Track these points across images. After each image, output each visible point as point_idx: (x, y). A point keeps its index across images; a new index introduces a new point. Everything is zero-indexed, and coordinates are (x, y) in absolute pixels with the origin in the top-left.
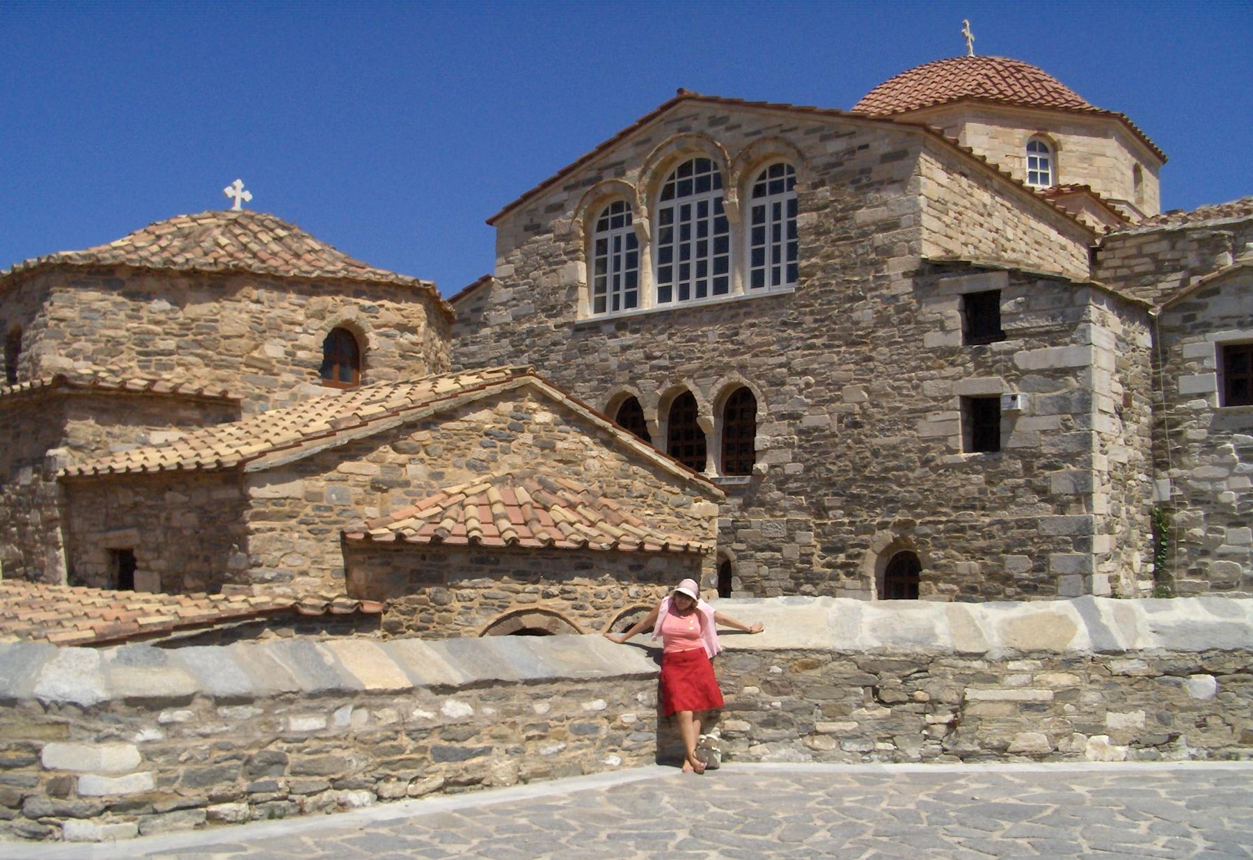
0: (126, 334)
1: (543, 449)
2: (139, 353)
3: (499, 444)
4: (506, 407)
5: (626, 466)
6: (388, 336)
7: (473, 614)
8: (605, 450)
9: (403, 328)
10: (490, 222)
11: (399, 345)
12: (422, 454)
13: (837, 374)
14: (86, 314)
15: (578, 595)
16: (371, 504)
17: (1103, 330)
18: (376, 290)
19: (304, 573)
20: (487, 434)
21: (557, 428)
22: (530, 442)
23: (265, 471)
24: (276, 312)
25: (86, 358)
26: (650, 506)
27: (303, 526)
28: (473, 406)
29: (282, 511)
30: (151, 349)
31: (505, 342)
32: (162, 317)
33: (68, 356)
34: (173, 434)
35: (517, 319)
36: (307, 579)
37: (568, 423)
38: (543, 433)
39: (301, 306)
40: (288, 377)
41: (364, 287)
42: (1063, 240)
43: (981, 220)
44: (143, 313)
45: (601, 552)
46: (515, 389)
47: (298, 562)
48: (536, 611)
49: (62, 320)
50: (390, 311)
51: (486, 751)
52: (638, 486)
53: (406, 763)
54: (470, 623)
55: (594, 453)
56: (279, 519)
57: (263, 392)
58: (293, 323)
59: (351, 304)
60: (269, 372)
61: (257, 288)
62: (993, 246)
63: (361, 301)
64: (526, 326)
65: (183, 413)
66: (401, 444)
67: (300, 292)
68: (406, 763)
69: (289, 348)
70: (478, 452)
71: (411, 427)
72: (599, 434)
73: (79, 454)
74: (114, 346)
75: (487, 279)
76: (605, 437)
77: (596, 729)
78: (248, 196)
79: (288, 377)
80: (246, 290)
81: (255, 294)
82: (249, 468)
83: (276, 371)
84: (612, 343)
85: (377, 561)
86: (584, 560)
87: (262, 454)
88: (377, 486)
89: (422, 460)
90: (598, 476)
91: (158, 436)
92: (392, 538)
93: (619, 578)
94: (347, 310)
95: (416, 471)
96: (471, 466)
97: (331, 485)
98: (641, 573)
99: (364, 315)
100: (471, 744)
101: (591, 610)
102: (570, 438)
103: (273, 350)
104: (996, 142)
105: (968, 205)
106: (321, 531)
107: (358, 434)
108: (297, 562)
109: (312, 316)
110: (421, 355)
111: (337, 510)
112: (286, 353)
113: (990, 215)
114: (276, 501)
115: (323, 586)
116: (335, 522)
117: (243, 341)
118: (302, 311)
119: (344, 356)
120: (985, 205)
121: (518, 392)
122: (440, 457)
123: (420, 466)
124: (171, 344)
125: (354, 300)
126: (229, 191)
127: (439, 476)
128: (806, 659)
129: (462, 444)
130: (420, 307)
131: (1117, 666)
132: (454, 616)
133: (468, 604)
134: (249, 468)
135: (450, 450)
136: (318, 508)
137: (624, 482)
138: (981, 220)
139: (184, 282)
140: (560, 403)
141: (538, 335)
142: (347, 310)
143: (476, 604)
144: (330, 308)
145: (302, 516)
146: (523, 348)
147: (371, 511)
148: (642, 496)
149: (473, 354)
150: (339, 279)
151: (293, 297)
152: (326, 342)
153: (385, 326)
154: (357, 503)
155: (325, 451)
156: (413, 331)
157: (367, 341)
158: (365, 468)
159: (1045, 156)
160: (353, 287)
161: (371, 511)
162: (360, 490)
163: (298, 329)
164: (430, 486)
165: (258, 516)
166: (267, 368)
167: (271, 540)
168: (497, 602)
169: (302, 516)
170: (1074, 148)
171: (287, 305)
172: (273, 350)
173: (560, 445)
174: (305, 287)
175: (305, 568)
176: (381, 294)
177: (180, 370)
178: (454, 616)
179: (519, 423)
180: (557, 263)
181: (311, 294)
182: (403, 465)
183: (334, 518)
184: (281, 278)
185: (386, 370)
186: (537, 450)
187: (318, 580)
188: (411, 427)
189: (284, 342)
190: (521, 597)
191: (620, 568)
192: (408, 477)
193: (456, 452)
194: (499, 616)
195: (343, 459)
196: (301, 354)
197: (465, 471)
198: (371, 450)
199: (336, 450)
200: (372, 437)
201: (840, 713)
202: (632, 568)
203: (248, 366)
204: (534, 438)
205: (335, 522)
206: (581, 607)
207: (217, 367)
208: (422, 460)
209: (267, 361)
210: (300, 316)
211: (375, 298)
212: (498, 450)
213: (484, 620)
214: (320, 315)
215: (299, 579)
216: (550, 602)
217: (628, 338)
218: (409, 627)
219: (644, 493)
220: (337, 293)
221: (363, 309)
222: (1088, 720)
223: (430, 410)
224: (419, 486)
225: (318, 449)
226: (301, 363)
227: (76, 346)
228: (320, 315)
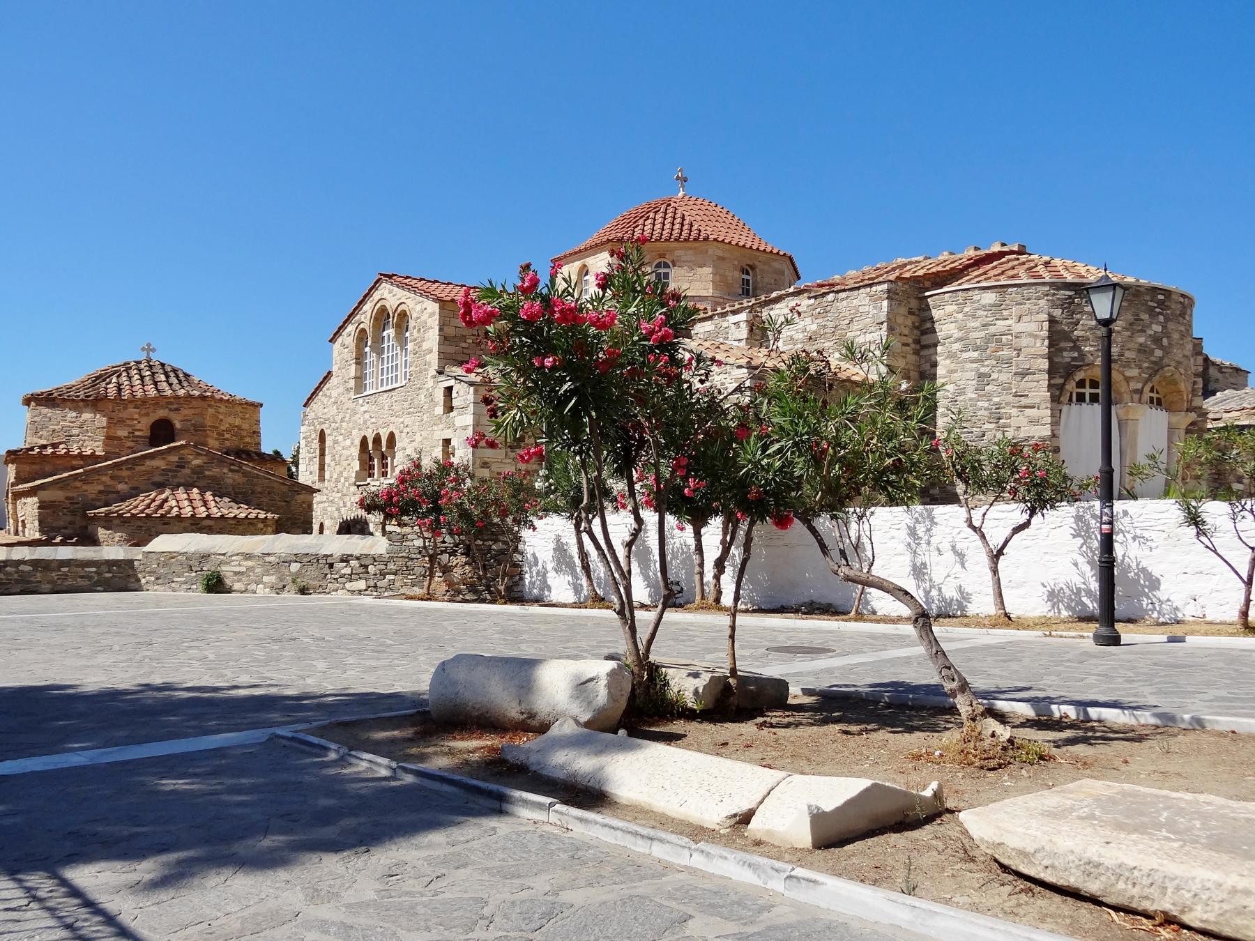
52: (259, 489)
103: (122, 433)
128: (171, 555)
131: (268, 559)
139: (81, 404)
159: (666, 270)
196: (137, 433)
210: (136, 416)
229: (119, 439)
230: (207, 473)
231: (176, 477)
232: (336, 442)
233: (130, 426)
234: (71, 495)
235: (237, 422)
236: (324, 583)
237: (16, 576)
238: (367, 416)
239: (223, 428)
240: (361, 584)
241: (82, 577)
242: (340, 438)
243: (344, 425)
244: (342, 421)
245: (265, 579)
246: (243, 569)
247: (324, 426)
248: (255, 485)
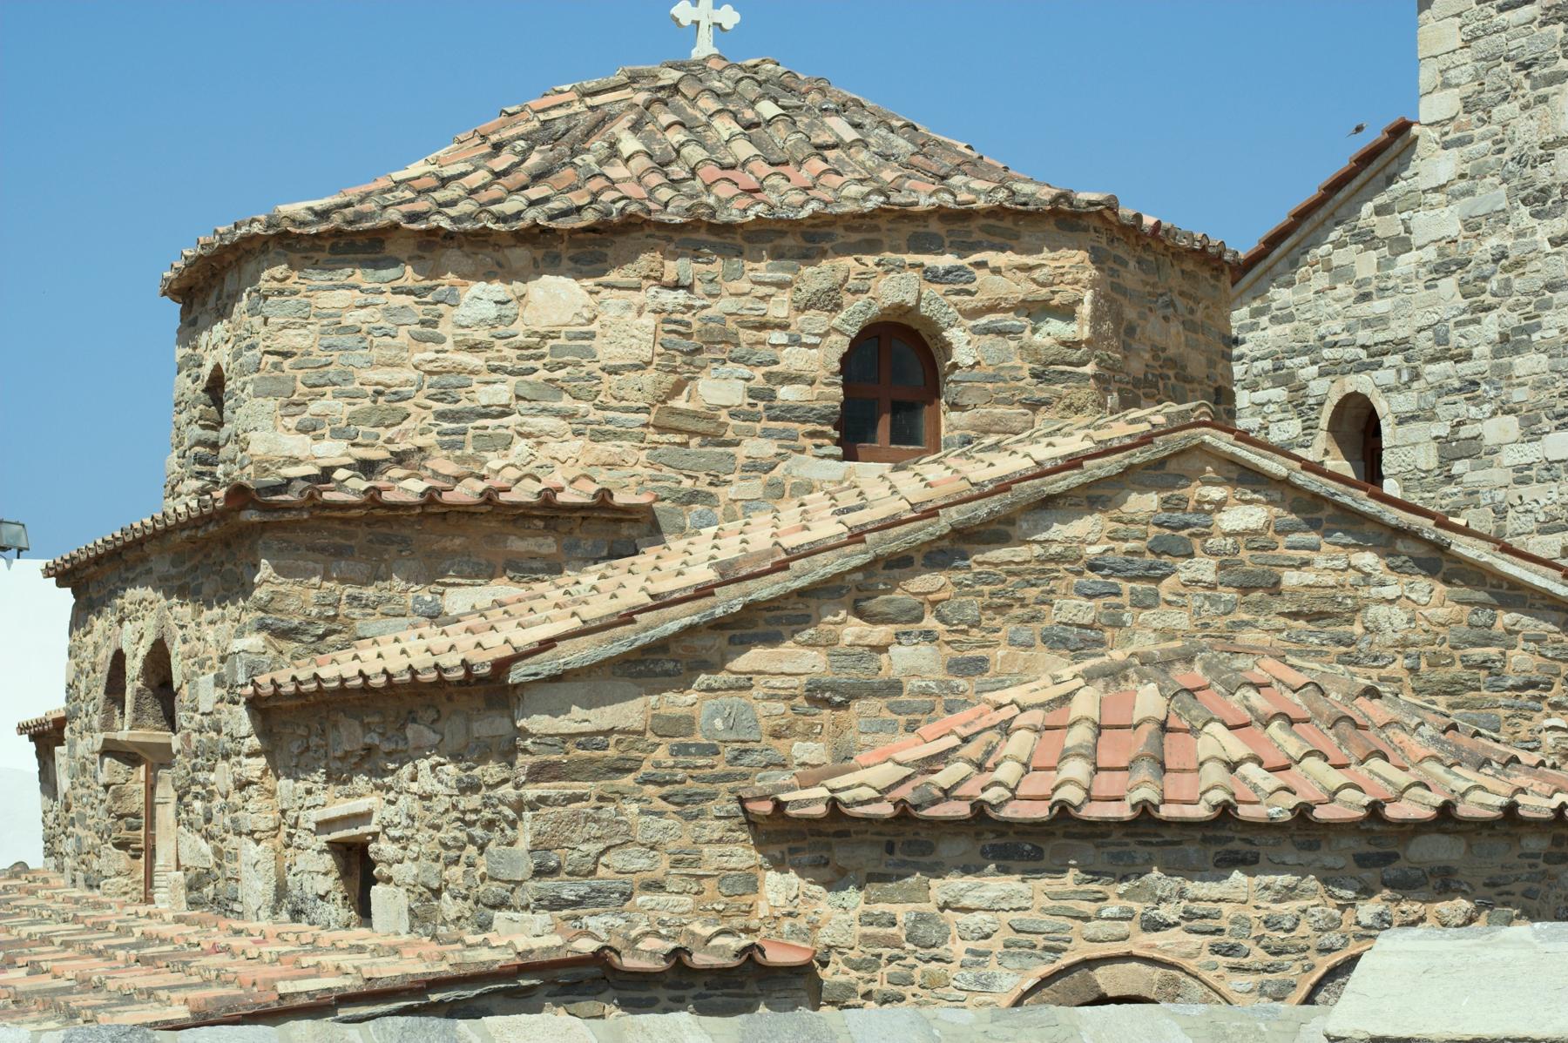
0: (414, 375)
1: (1245, 589)
2: (441, 416)
3: (1126, 587)
4: (1143, 503)
5: (1483, 617)
6: (1000, 332)
7: (992, 967)
8: (1422, 583)
9: (1037, 310)
11: (1030, 352)
12: (930, 622)
14: (334, 339)
15: (1223, 923)
16: (808, 735)
18: (961, 228)
19: (656, 886)
20: (1093, 567)
21: (1283, 541)
22: (1210, 577)
23: (554, 679)
25: (337, 434)
26: (1556, 706)
27: (650, 789)
28: (1048, 505)
30: (464, 404)
31: (1448, 285)
32: (482, 335)
33: (303, 430)
34: (502, 589)
35: (1471, 225)
36: (661, 898)
37: (1314, 525)
38: (1244, 554)
39: (781, 285)
40: (758, 448)
41: (935, 226)
44: (444, 329)
45: (1271, 826)
46: (1161, 463)
47: (643, 863)
48: (1129, 957)
49: (286, 355)
50: (1002, 274)
52: (1521, 660)
54: (986, 985)
55: (1389, 592)
56: (595, 776)
57: (702, 485)
58: (762, 326)
59: (902, 267)
60: (714, 438)
61: (675, 256)
63: (928, 260)
64: (1491, 243)
65: (518, 545)
66: (875, 605)
67: (778, 255)
69: (759, 381)
70: (1073, 608)
71: (900, 563)
72: (1400, 545)
73: (290, 646)
74: (388, 404)
75: (1401, 130)
76: (1421, 551)
78: (729, 17)
79: (758, 448)
80: (646, 261)
81: (674, 268)
82: (515, 676)
83: (729, 435)
85: (805, 857)
86: (1236, 845)
87: (548, 644)
88: (820, 696)
89: (928, 635)
90: (1404, 644)
91: (459, 599)
92: (819, 810)
93: (1329, 879)
94: (891, 282)
95: (911, 660)
96: (1055, 641)
97: (711, 701)
98: (1392, 871)
99: (937, 290)
101: (1258, 956)
102: (1320, 560)
103: (719, 389)
106: (690, 798)
107: (764, 590)
108: (637, 861)
110: (1089, 369)
111: (727, 752)
112: (753, 393)
114: (587, 739)
115: (700, 912)
116: (727, 777)
117: (650, 376)
118: (786, 296)
119: (890, 390)
121: (1172, 466)
122: (976, 624)
123: (925, 649)
124: (501, 392)
125: (910, 258)
127: (977, 666)
129: (1032, 593)
130: (1081, 255)
132: (953, 970)
133: (982, 945)
134: (515, 676)
135: (1000, 609)
136: (682, 750)
137: (1477, 653)
139: (520, 255)
140: (1285, 482)
141: (1518, 264)
142: (891, 282)
143: (996, 944)
144: (852, 283)
145: (647, 768)
146: (1488, 299)
147: (809, 751)
148: (1531, 685)
149: (1382, 320)
150: (873, 214)
151: (764, 269)
152: (845, 360)
153: (992, 309)
154: (776, 735)
155: (690, 630)
156: (1067, 313)
157: (947, 347)
158: (794, 661)
160: (908, 229)
161: (809, 751)
162: (781, 707)
163: (778, 337)
164: (953, 690)
166: (710, 430)
167: (574, 819)
168: (1040, 941)
169: (647, 768)
171: (743, 288)
172: (719, 389)
173: (1291, 578)
174: (789, 242)
175: (658, 874)
176: (977, 236)
177: (521, 446)
178: (953, 970)
179: (1175, 541)
180: (1551, 80)
181: (809, 255)
182: (882, 649)
183: (722, 768)
184: (729, 227)
185: (1000, 410)
186: (1229, 594)
187: (688, 901)
188: (900, 563)
189: (745, 371)
190: (1091, 928)
191: (1329, 861)
192: (894, 674)
193: (1017, 611)
194: (1045, 969)
195: (744, 643)
196: (788, 394)
197: (1042, 653)
198: (805, 620)
199: (717, 625)
200: (801, 593)
202: (1362, 861)
203: (662, 429)
204: (1222, 567)
205: (727, 777)
206: (1231, 950)
207: (599, 436)
208: (928, 635)
209: (709, 415)
210: (779, 308)
211: (963, 248)
212: (1125, 599)
213: (1013, 980)
214: (829, 301)
215: (641, 899)
216: (1159, 939)
218: (867, 995)
219: (1536, 676)
220: (872, 247)
221: (933, 276)
223: (943, 524)
224: (925, 692)
225: (673, 627)
226: (789, 413)
227: (315, 407)
228: (829, 301)
232: (1456, 448)
235: (1174, 338)
242: (1499, 430)
243: (1527, 364)
244: (1509, 343)
247: (1361, 383)
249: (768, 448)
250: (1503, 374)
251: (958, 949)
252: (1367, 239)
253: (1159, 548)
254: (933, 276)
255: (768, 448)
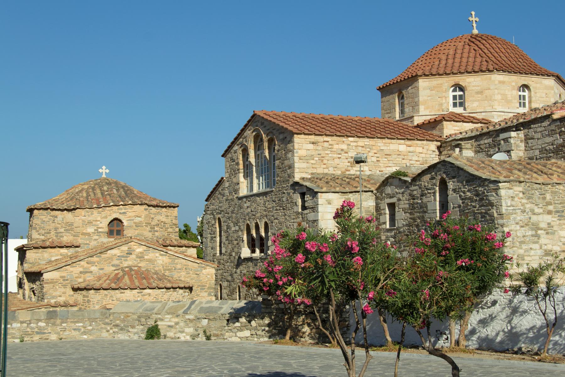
10: (223, 156)
13: (281, 220)
17: (330, 206)
19: (60, 296)
24: (90, 219)
29: (52, 282)
32: (60, 222)
42: (411, 149)
43: (340, 156)
51: (50, 333)
52: (179, 266)
53: (29, 334)
57: (88, 242)
62: (349, 164)
68: (29, 334)
77: (80, 330)
78: (108, 171)
79: (96, 237)
84: (245, 205)
89: (96, 266)
100: (46, 331)
103: (90, 230)
104: (434, 92)
105: (329, 152)
109: (103, 218)
113: (346, 153)
120: (342, 150)
124: (62, 230)
126: (100, 171)
136: (64, 280)
138: (340, 156)
163: (99, 222)
165: (47, 283)
170: (474, 88)
173: (146, 257)
196: (100, 230)
201: (133, 327)
207: (74, 236)
210: (99, 219)
217: (248, 204)
221: (120, 213)
222: (181, 330)
226: (100, 232)
229: (89, 234)
230: (146, 257)
231: (126, 260)
233: (95, 225)
234: (63, 275)
236: (223, 332)
237: (36, 330)
238: (249, 210)
239: (153, 223)
240: (247, 333)
241: (74, 330)
243: (234, 215)
244: (232, 212)
245: (187, 330)
246: (173, 324)
248: (177, 264)
249: (97, 237)
250: (232, 217)
251: (91, 303)
252: (220, 193)
253: (127, 254)
254: (120, 213)
255: (97, 237)
